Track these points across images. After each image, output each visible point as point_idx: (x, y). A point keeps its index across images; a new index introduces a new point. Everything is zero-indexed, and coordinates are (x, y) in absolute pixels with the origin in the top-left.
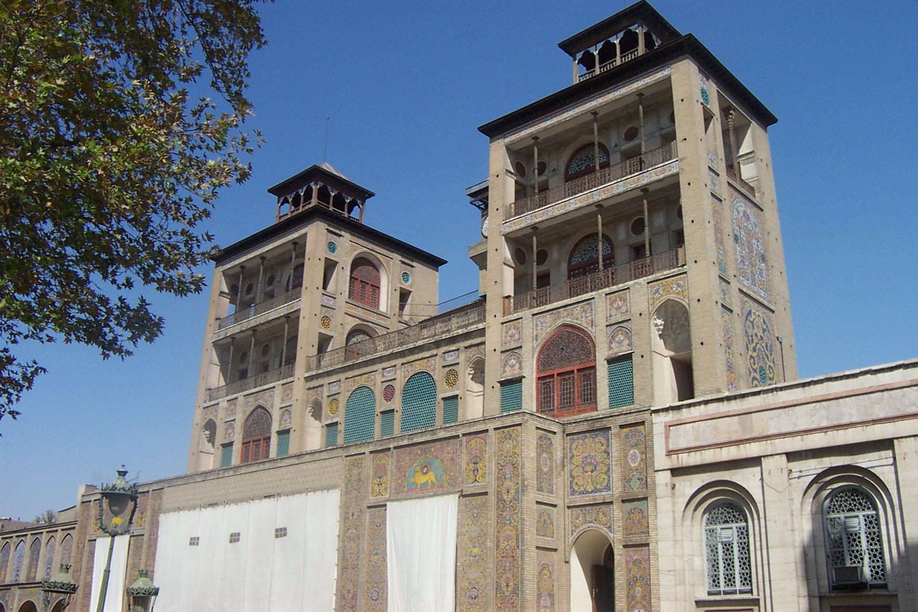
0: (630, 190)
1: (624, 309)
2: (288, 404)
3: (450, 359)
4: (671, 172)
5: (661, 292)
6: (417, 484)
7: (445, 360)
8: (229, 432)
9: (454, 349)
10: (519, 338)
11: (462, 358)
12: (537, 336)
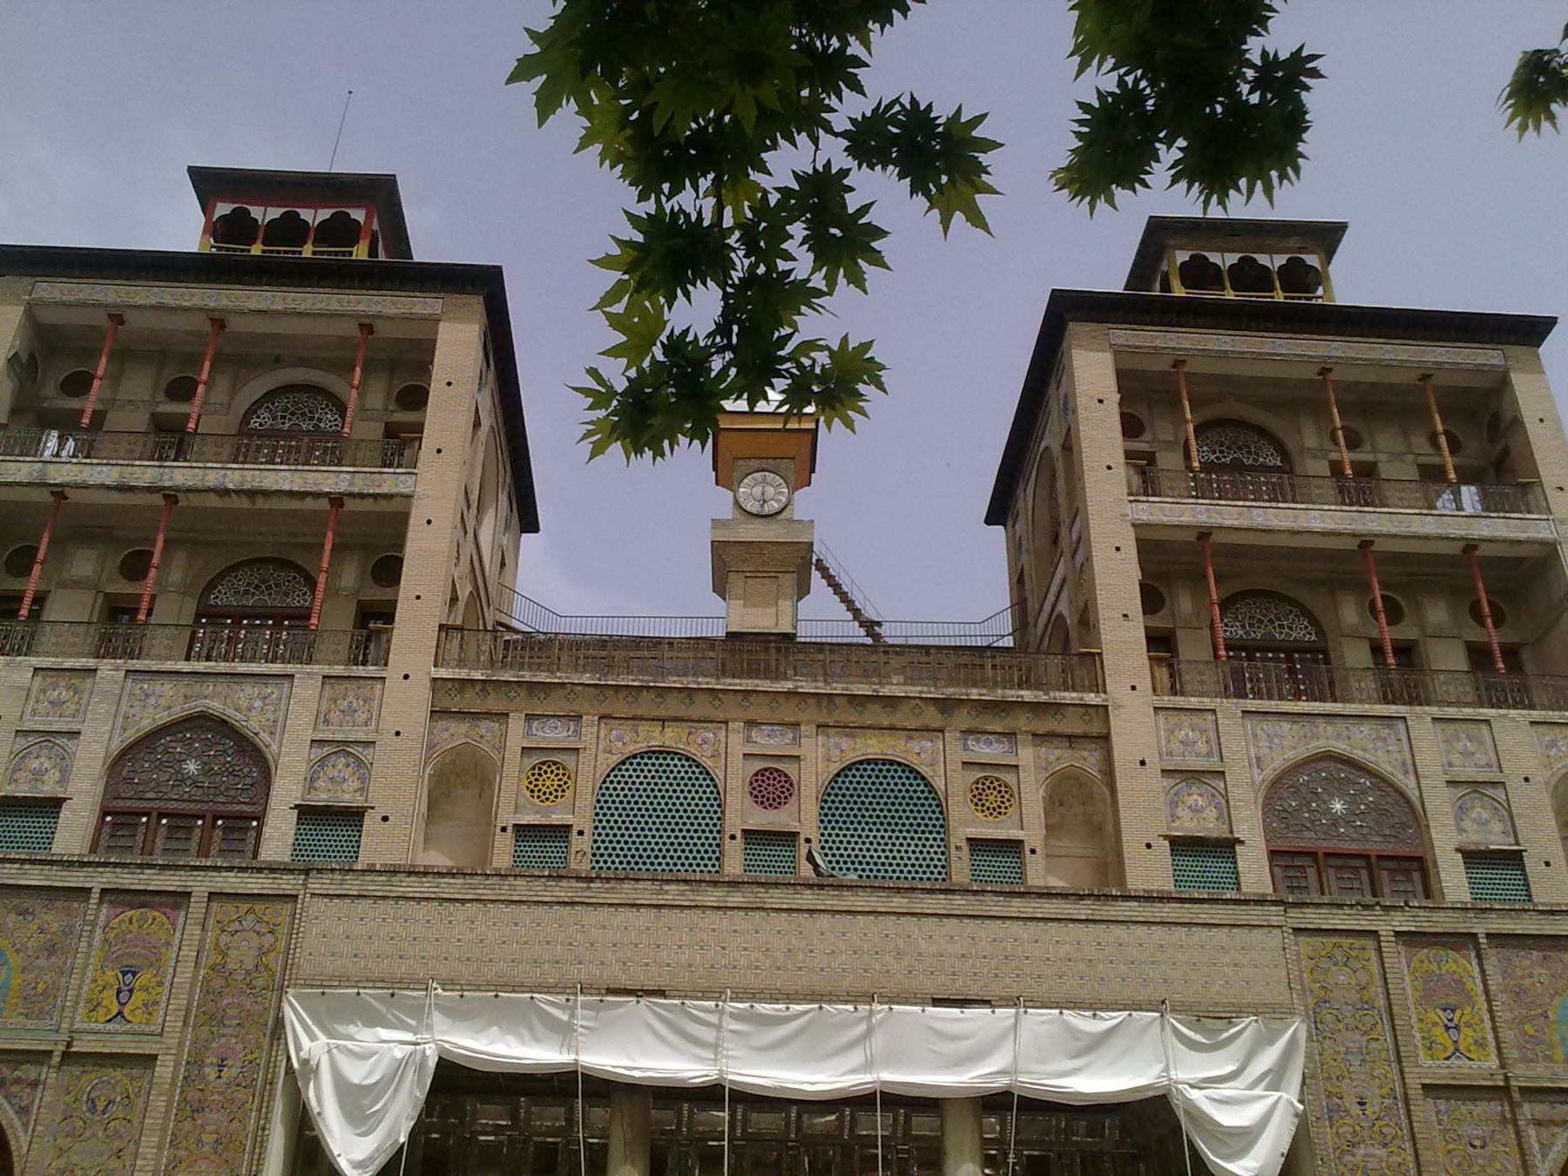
0: (1454, 539)
1: (1480, 758)
2: (362, 737)
4: (1541, 536)
7: (966, 748)
8: (35, 764)
10: (1209, 754)
11: (1026, 755)
12: (1258, 759)
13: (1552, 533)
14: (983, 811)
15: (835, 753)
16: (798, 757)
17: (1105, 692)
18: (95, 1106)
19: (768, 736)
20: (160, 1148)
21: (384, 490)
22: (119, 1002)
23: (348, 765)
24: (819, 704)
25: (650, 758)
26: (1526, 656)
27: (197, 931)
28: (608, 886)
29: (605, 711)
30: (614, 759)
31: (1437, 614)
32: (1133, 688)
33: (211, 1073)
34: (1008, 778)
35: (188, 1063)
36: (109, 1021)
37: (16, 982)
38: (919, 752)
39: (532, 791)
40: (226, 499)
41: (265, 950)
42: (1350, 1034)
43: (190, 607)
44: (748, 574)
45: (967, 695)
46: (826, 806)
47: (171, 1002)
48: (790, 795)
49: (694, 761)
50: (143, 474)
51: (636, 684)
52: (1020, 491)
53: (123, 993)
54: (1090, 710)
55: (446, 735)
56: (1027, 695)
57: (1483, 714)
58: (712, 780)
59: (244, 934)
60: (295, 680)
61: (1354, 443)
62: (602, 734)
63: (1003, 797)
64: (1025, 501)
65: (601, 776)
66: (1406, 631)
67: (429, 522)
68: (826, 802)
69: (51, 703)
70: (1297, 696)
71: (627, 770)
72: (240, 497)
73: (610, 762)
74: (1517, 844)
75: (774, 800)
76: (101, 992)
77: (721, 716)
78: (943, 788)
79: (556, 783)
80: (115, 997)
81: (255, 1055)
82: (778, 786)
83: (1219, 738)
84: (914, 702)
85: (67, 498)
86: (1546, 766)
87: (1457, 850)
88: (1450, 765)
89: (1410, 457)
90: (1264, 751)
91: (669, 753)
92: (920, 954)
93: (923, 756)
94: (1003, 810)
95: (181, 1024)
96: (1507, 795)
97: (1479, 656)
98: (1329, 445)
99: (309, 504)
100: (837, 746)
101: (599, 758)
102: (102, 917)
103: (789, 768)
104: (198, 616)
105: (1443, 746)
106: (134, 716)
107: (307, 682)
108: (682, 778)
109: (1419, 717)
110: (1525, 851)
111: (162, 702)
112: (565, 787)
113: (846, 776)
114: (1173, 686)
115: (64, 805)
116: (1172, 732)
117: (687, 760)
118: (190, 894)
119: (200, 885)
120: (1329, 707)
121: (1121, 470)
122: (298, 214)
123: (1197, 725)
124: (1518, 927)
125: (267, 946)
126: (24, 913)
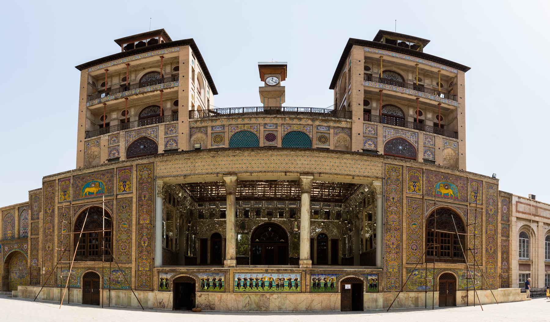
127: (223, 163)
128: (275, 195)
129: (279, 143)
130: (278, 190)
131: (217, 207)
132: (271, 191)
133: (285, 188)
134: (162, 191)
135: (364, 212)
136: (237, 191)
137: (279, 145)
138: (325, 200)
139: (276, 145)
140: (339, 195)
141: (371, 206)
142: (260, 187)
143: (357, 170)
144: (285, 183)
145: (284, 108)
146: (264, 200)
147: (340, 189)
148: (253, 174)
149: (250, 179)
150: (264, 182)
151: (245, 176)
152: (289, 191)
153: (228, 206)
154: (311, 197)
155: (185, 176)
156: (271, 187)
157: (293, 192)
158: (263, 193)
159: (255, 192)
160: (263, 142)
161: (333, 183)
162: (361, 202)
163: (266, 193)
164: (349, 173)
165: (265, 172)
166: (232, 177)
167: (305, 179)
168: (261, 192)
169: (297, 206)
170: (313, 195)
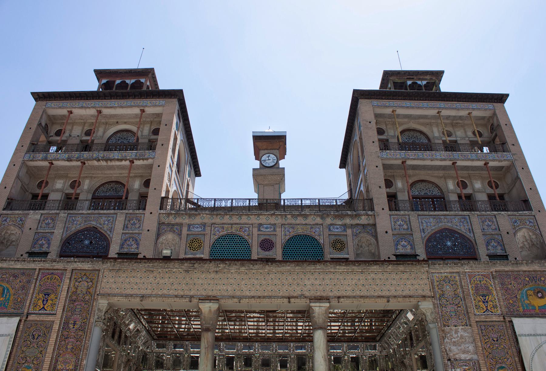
1: (494, 227)
2: (137, 231)
3: (336, 230)
5: (519, 223)
6: (534, 306)
7: (330, 230)
8: (41, 242)
9: (340, 223)
10: (408, 229)
11: (349, 232)
12: (423, 230)
13: (511, 158)
14: (336, 250)
15: (287, 233)
16: (276, 234)
17: (374, 211)
18: (34, 337)
19: (266, 228)
20: (54, 350)
21: (146, 157)
22: (43, 304)
23: (133, 240)
24: (282, 218)
25: (228, 236)
26: (506, 197)
27: (68, 281)
28: (200, 265)
29: (213, 221)
30: (216, 237)
31: (478, 185)
32: (383, 209)
33: (71, 326)
34: (343, 239)
35: (64, 323)
36: (40, 310)
37: (12, 298)
38: (315, 233)
39: (190, 248)
40: (99, 162)
41: (89, 287)
42: (451, 305)
43: (90, 197)
44: (264, 185)
45: (330, 213)
46: (285, 250)
47: (59, 303)
48: (273, 247)
49: (242, 237)
50: (75, 156)
51: (223, 213)
52: (349, 157)
53: (45, 301)
54: (369, 217)
55: (163, 231)
56: (349, 213)
57: (493, 213)
58: (248, 243)
59: (83, 282)
60: (118, 215)
61: (449, 135)
62: (213, 229)
63: (342, 245)
64: (350, 159)
65: (212, 242)
66: (468, 191)
67: (159, 166)
68: (285, 248)
69: (46, 224)
70: (435, 210)
71: (220, 240)
72: (103, 161)
73: (215, 238)
74: (506, 253)
75: (268, 248)
76: (38, 301)
77: (250, 222)
78: (322, 242)
79: (198, 245)
80: (42, 303)
81: (85, 320)
82: (269, 244)
83: (410, 224)
84: (312, 217)
85: (53, 164)
86: (513, 229)
87: (487, 255)
88: (484, 229)
89: (467, 139)
90: (425, 227)
91: (234, 235)
92: (305, 285)
93: (316, 233)
94: (342, 249)
95: (62, 311)
96: (502, 238)
97: (491, 197)
98: (442, 135)
99: (123, 163)
100: (288, 231)
101: (211, 237)
102: (39, 278)
103: (273, 238)
104: (92, 199)
105: (481, 224)
106: (70, 227)
107: (120, 217)
108: (238, 243)
109: (473, 215)
110: (509, 255)
111: (78, 223)
112: (201, 246)
113: (291, 240)
114: (396, 208)
115: (49, 254)
116: (396, 223)
117: (240, 237)
118: (66, 270)
119: (70, 267)
120: (445, 212)
121: (377, 144)
122: (125, 81)
123: (404, 220)
124: (506, 268)
125: (90, 286)
126: (15, 276)
127: (200, 281)
128: (274, 333)
129: (278, 253)
130: (279, 326)
131: (186, 350)
132: (268, 328)
133: (288, 322)
134: (103, 317)
135: (412, 355)
136: (218, 327)
137: (279, 257)
138: (350, 340)
139: (274, 256)
140: (370, 331)
141: (422, 344)
142: (251, 321)
143: (392, 288)
144: (288, 315)
145: (284, 200)
146: (257, 341)
147: (371, 321)
148: (241, 301)
149: (237, 309)
150: (258, 313)
151: (230, 304)
152: (294, 328)
153: (203, 350)
154: (328, 336)
155: (143, 297)
156: (268, 321)
157: (301, 328)
158: (255, 331)
159: (244, 329)
160: (256, 252)
161: (359, 312)
162: (406, 339)
163: (260, 331)
164: (380, 294)
165: (259, 297)
166: (211, 304)
167: (318, 308)
168: (253, 329)
169: (308, 351)
170: (331, 333)
